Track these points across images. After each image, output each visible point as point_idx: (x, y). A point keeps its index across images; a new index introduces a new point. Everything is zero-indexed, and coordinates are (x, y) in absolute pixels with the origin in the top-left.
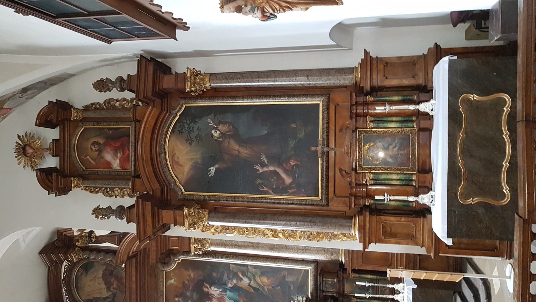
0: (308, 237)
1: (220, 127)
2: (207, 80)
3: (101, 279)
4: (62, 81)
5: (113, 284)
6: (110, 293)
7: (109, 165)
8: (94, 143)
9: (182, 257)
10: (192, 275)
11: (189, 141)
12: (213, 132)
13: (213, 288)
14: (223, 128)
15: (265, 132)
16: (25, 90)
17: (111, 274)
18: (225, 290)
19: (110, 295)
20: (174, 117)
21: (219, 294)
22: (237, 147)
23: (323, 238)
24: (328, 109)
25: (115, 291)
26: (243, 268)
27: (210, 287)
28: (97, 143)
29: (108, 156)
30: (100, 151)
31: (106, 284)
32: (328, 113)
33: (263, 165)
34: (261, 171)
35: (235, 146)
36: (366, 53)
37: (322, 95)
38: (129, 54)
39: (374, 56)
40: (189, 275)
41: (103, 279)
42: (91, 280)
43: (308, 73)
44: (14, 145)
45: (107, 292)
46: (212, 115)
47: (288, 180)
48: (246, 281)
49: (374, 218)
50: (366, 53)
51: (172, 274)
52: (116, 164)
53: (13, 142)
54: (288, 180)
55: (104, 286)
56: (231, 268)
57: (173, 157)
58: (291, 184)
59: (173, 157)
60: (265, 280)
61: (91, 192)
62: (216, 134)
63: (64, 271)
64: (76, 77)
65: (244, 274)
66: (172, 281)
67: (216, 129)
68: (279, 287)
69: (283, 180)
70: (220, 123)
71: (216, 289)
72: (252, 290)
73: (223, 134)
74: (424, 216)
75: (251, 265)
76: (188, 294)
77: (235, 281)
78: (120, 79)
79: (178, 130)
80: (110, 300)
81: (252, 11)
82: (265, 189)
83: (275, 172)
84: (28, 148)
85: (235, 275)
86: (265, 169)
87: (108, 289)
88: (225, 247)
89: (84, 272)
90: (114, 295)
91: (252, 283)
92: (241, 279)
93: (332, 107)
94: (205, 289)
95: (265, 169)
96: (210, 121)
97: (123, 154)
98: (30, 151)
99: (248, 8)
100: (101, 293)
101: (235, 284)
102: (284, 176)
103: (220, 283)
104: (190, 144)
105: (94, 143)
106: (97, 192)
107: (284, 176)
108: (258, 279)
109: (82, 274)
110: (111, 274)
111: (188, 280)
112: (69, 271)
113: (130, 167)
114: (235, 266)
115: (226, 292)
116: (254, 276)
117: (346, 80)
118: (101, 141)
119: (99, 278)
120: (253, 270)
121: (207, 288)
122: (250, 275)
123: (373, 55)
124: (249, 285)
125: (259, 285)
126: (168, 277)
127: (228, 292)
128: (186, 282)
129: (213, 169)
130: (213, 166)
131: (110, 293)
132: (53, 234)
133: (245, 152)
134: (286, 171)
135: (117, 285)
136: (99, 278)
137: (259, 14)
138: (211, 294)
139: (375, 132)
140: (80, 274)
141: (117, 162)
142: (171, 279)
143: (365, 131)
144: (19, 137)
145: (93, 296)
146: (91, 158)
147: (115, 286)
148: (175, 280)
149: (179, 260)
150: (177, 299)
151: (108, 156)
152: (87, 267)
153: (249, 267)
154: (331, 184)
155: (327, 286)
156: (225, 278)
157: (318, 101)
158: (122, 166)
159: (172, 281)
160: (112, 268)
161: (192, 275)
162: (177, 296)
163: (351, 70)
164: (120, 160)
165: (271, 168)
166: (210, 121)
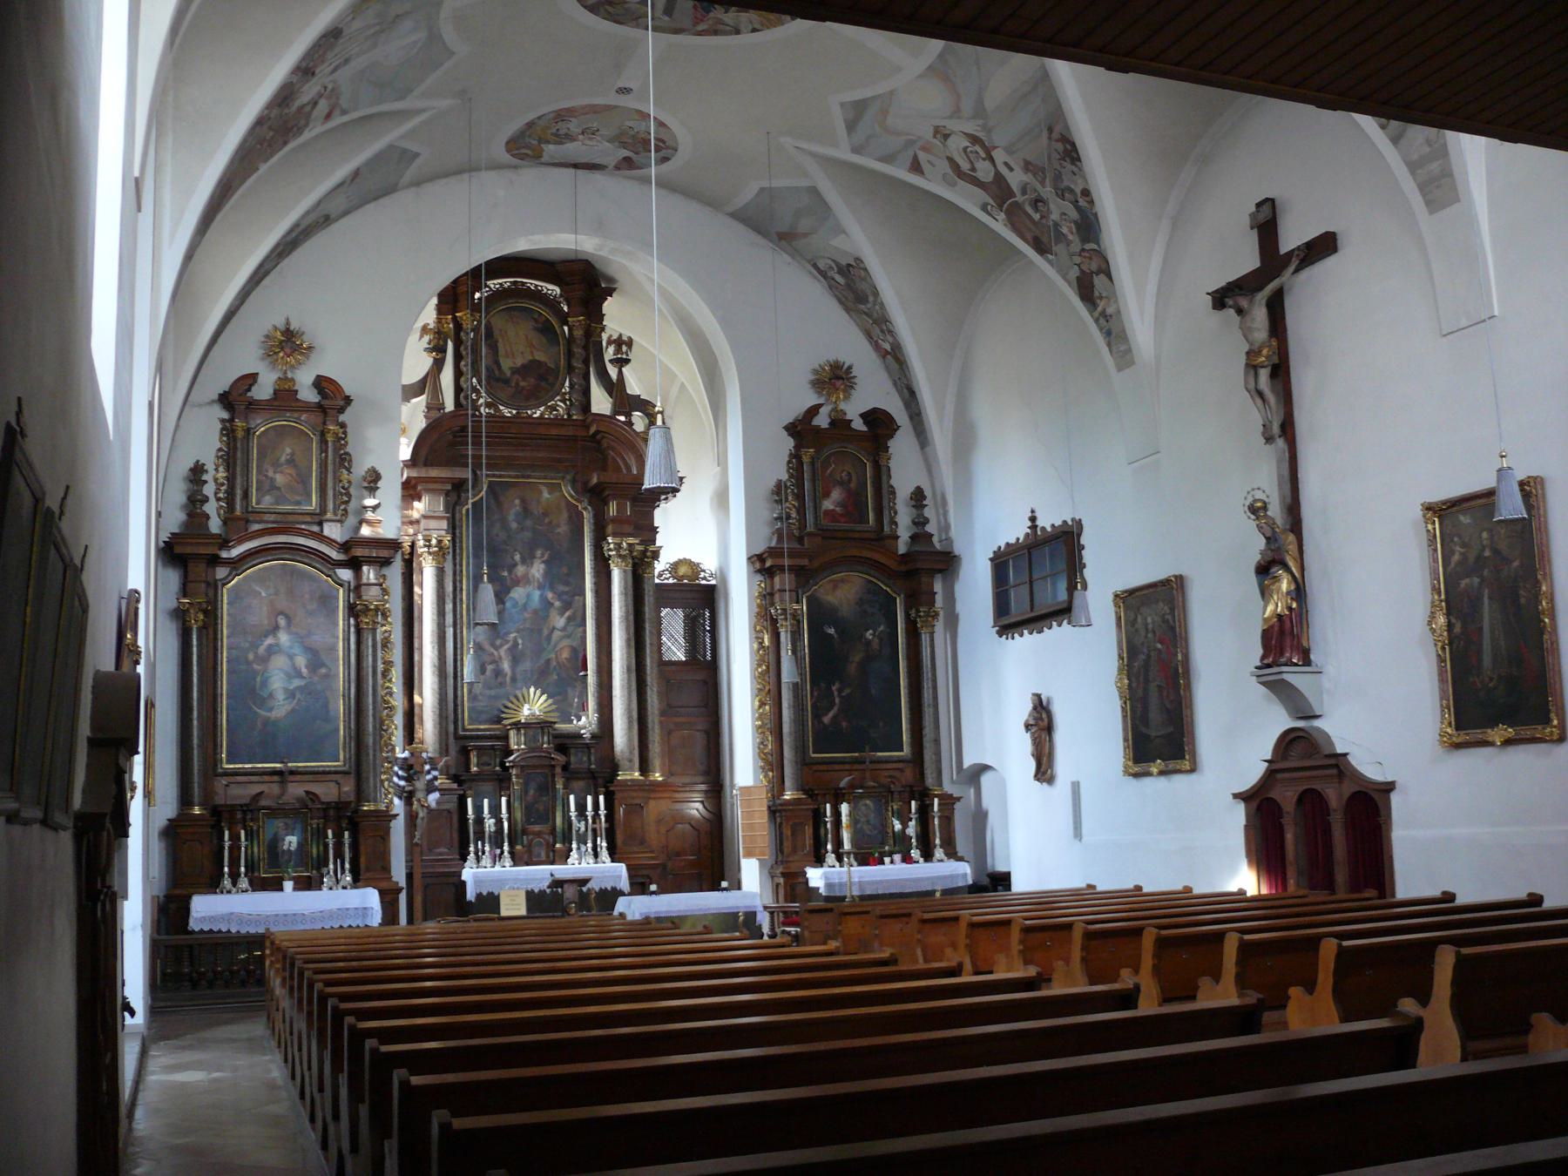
0: (762, 743)
1: (876, 640)
2: (930, 629)
3: (531, 358)
4: (915, 429)
5: (524, 379)
6: (508, 373)
7: (827, 495)
8: (849, 474)
9: (588, 517)
10: (559, 530)
11: (861, 602)
12: (871, 631)
13: (543, 566)
14: (875, 645)
15: (873, 692)
16: (912, 393)
17: (542, 378)
18: (540, 587)
19: (505, 374)
20: (885, 585)
21: (533, 576)
22: (857, 659)
23: (763, 759)
24: (900, 761)
25: (513, 384)
26: (579, 619)
27: (543, 562)
28: (850, 481)
29: (836, 494)
30: (841, 483)
31: (524, 366)
32: (896, 762)
33: (840, 691)
34: (834, 688)
35: (857, 657)
36: (959, 799)
37: (913, 754)
38: (953, 533)
39: (955, 806)
40: (558, 526)
41: (530, 361)
42: (527, 337)
43: (937, 741)
44: (841, 359)
45: (511, 368)
46: (888, 630)
47: (826, 720)
48: (560, 622)
49: (810, 814)
50: (959, 799)
51: (558, 494)
52: (828, 505)
53: (846, 358)
54: (826, 720)
55: (519, 362)
56: (577, 598)
57: (842, 581)
58: (822, 722)
59: (842, 581)
60: (565, 655)
61: (789, 462)
62: (869, 635)
63: (536, 286)
64: (918, 448)
65: (569, 619)
66: (546, 495)
67: (874, 635)
68: (556, 677)
69: (826, 715)
70: (881, 639)
71: (541, 571)
72: (546, 632)
73: (869, 643)
74: (816, 862)
75: (585, 632)
76: (528, 523)
77: (557, 604)
78: (927, 521)
79: (872, 590)
80: (497, 372)
81: (1035, 719)
82: (816, 694)
83: (832, 705)
84: (841, 382)
85: (567, 606)
86: (836, 693)
87: (515, 371)
88: (621, 594)
89: (540, 326)
90: (506, 382)
91: (557, 634)
92: (562, 614)
93: (900, 765)
94: (539, 553)
95: (836, 693)
96: (882, 628)
97: (841, 515)
98: (839, 383)
99: (1036, 715)
100: (507, 356)
101: (552, 604)
102: (831, 714)
103: (551, 579)
104: (857, 604)
105: (849, 474)
106: (788, 471)
107: (831, 714)
108: (566, 642)
109: (536, 320)
110: (542, 378)
111: (550, 522)
112: (538, 296)
113: (824, 522)
114: (581, 604)
115: (539, 588)
116: (568, 637)
117: (930, 780)
118: (853, 485)
119: (532, 352)
120: (579, 635)
121: (543, 555)
122: (570, 629)
123: (957, 806)
124: (554, 628)
125: (555, 646)
126: (553, 488)
127: (536, 594)
128: (547, 520)
129: (831, 631)
130: (836, 631)
131: (508, 373)
132: (611, 280)
133: (852, 668)
134: (835, 717)
135: (523, 387)
136: (532, 352)
137: (1032, 722)
138: (532, 564)
139: (887, 810)
140: (536, 316)
141: (832, 507)
142: (550, 493)
143: (887, 802)
144: (850, 368)
145: (500, 340)
146: (831, 472)
147: (522, 384)
148: (548, 499)
149: (585, 509)
150: (517, 502)
151: (836, 494)
152: (547, 330)
153: (581, 629)
154: (824, 767)
155: (580, 754)
156: (562, 588)
157: (906, 751)
158: (827, 512)
159: (546, 495)
160: (551, 380)
161: (559, 530)
162: (523, 501)
163: (940, 785)
164: (833, 510)
165: (837, 700)
166: (882, 628)
